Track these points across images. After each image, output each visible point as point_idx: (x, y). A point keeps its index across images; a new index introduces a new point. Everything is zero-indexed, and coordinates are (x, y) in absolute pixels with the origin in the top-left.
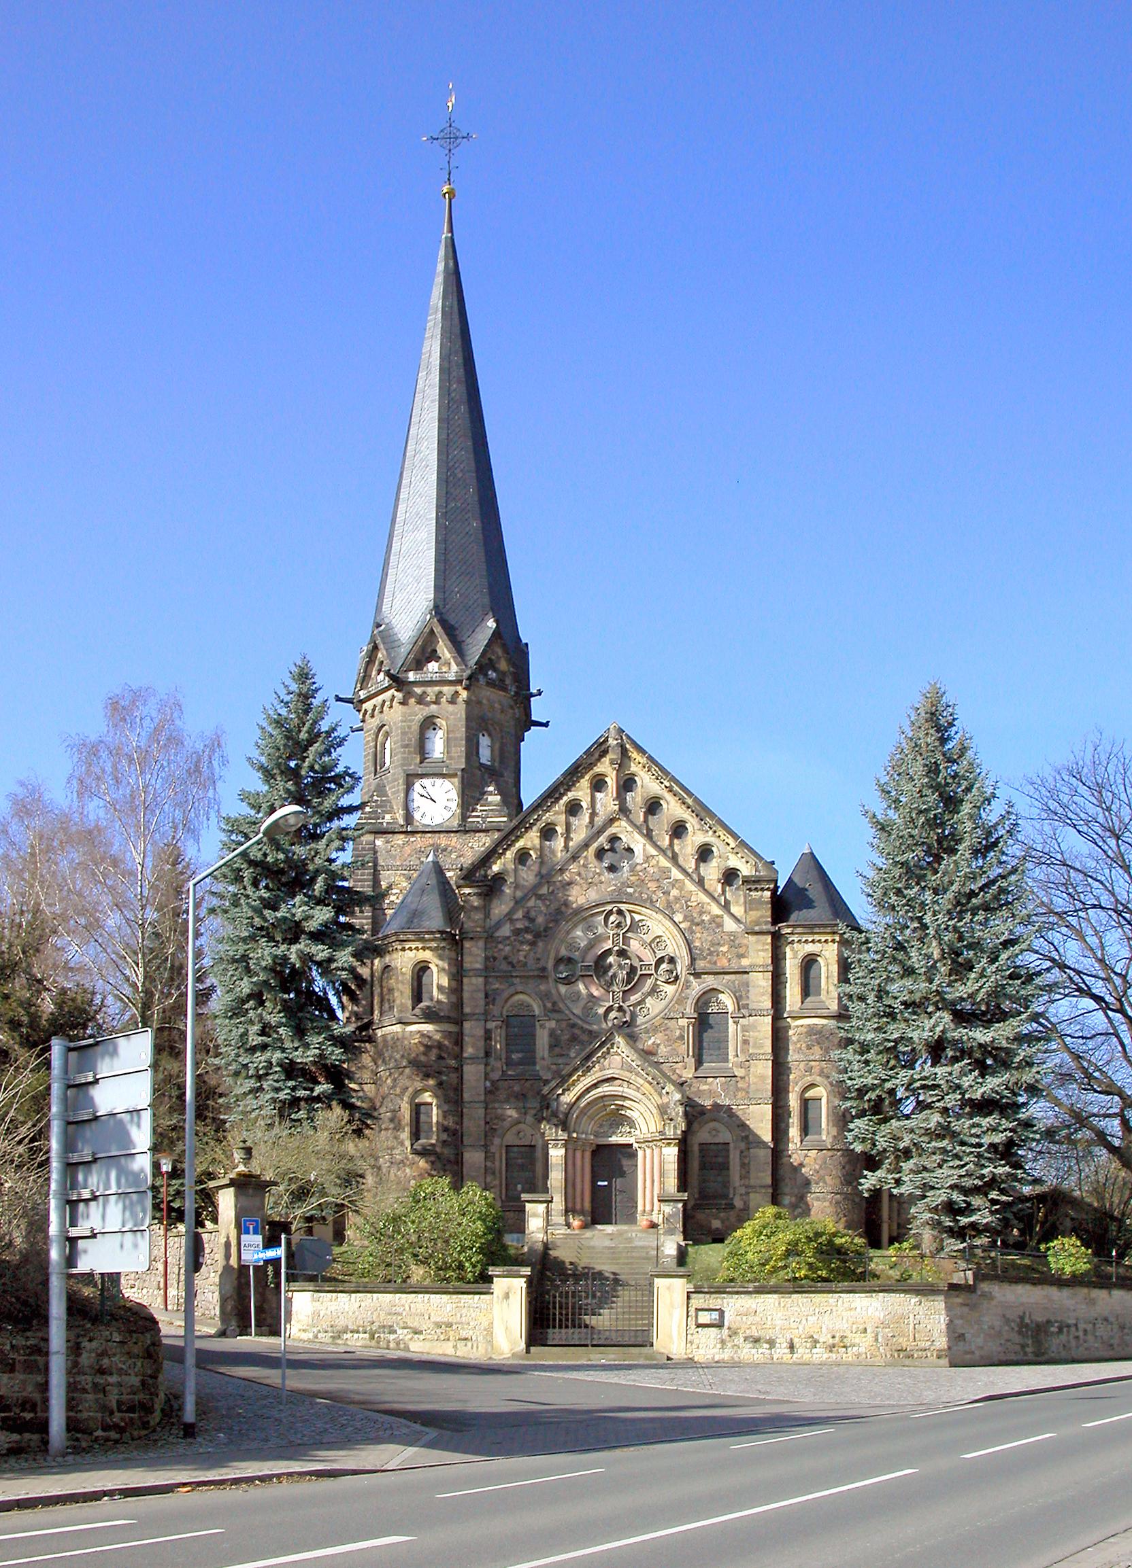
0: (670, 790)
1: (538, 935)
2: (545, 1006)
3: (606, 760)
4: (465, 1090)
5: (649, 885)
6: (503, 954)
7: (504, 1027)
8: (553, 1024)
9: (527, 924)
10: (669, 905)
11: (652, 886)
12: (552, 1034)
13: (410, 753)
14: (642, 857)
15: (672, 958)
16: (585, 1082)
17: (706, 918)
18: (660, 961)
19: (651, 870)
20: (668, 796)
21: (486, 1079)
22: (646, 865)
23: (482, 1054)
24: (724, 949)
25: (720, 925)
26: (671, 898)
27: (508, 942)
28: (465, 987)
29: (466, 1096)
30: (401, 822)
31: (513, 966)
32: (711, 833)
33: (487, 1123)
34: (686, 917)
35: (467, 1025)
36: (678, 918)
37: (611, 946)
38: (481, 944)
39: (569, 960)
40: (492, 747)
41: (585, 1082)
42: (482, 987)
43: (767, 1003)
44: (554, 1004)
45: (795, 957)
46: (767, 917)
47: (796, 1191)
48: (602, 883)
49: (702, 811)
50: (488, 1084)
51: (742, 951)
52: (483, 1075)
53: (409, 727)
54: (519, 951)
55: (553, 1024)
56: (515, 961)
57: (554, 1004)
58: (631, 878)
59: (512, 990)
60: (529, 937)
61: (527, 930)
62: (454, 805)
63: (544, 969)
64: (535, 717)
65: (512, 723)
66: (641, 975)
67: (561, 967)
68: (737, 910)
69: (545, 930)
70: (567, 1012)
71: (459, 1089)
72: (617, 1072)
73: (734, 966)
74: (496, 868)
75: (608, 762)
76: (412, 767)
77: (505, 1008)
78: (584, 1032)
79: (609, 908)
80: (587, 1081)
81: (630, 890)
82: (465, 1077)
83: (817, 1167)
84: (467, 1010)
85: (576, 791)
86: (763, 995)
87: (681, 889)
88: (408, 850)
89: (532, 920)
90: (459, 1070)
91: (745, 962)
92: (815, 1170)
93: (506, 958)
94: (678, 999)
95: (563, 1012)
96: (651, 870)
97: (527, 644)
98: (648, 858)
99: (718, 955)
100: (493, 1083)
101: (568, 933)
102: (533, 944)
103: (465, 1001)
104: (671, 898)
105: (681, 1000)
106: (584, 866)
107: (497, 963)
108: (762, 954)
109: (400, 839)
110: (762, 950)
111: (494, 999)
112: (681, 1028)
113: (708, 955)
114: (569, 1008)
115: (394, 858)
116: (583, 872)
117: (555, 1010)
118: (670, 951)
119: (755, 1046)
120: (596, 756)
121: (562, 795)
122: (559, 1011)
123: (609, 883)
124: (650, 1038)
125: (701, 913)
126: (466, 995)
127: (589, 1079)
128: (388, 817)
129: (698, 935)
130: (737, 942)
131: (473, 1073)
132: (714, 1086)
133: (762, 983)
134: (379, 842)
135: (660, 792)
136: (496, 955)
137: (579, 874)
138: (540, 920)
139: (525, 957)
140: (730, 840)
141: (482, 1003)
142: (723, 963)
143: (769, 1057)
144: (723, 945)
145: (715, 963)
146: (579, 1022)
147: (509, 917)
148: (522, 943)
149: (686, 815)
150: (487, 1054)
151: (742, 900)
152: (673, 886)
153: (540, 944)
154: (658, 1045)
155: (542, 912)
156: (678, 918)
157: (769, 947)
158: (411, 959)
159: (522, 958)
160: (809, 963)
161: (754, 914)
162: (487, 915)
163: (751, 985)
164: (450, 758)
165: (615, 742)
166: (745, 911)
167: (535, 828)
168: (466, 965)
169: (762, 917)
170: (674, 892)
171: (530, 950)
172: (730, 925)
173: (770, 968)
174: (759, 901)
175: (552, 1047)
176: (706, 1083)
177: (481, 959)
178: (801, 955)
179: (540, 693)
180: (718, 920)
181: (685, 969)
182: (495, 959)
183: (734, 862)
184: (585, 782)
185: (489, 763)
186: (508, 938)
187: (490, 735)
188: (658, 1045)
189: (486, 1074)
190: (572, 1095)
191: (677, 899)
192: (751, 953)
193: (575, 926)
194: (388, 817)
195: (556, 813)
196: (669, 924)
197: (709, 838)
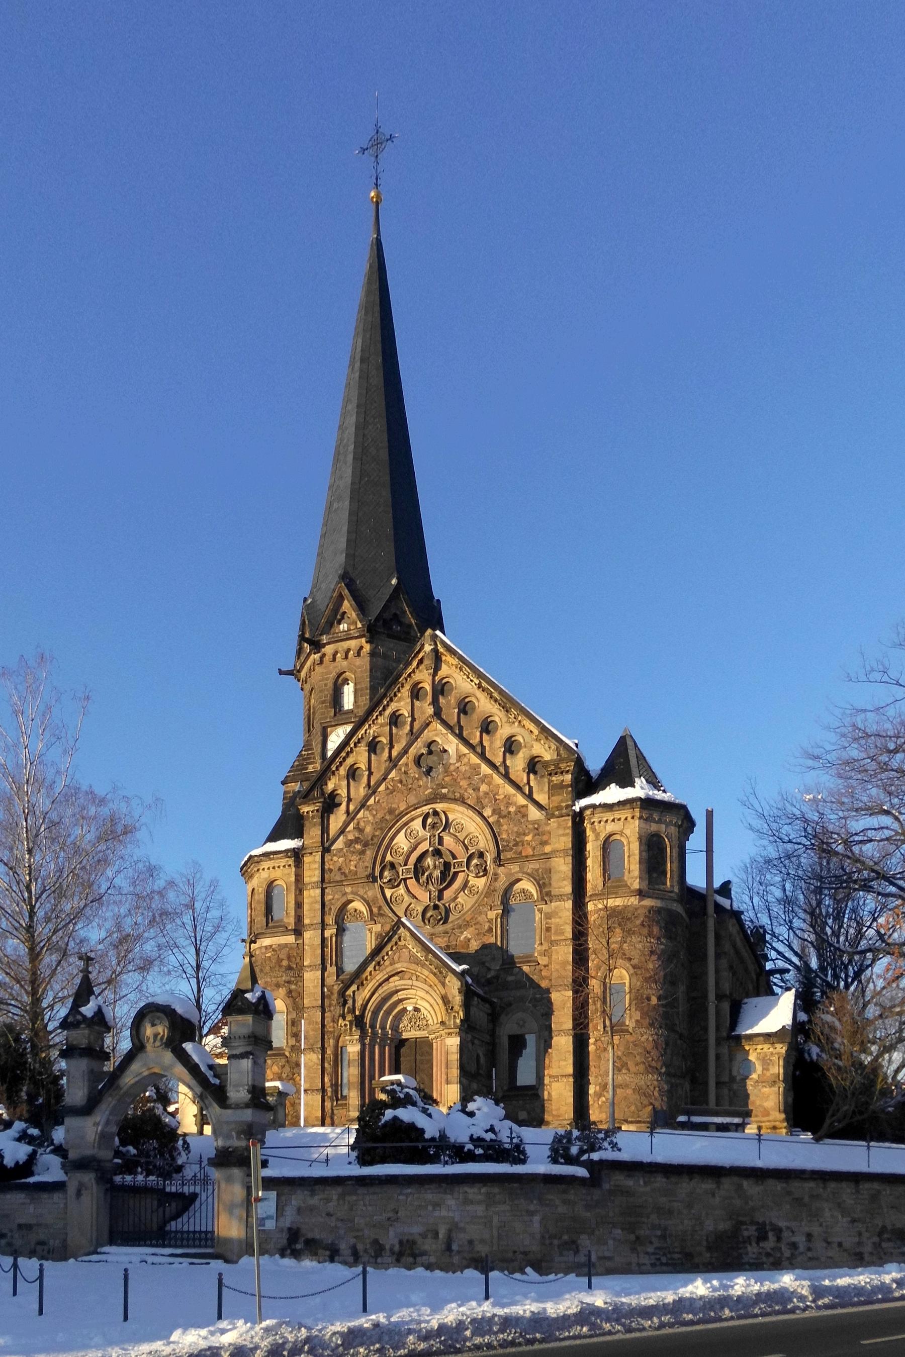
1: (366, 845)
6: (338, 865)
10: (479, 800)
11: (464, 783)
16: (378, 978)
17: (512, 809)
19: (463, 768)
24: (528, 838)
25: (525, 816)
26: (481, 794)
27: (341, 854)
34: (494, 811)
36: (487, 812)
43: (568, 889)
48: (420, 786)
51: (545, 838)
53: (326, 685)
58: (446, 779)
60: (358, 847)
61: (357, 840)
69: (372, 839)
79: (426, 809)
80: (380, 976)
81: (444, 791)
87: (489, 784)
91: (548, 849)
93: (340, 869)
96: (463, 768)
99: (523, 845)
102: (363, 852)
106: (406, 773)
107: (333, 874)
108: (563, 839)
110: (563, 835)
112: (490, 921)
119: (556, 934)
124: (462, 933)
125: (508, 804)
129: (505, 827)
130: (540, 830)
133: (563, 866)
137: (401, 782)
138: (368, 829)
139: (356, 867)
143: (569, 942)
147: (342, 831)
152: (483, 781)
154: (469, 940)
155: (369, 821)
159: (352, 868)
161: (556, 799)
166: (549, 798)
169: (562, 801)
171: (360, 859)
172: (534, 813)
174: (561, 786)
176: (512, 974)
182: (331, 870)
186: (342, 849)
188: (469, 940)
191: (486, 794)
192: (553, 840)
196: (478, 819)
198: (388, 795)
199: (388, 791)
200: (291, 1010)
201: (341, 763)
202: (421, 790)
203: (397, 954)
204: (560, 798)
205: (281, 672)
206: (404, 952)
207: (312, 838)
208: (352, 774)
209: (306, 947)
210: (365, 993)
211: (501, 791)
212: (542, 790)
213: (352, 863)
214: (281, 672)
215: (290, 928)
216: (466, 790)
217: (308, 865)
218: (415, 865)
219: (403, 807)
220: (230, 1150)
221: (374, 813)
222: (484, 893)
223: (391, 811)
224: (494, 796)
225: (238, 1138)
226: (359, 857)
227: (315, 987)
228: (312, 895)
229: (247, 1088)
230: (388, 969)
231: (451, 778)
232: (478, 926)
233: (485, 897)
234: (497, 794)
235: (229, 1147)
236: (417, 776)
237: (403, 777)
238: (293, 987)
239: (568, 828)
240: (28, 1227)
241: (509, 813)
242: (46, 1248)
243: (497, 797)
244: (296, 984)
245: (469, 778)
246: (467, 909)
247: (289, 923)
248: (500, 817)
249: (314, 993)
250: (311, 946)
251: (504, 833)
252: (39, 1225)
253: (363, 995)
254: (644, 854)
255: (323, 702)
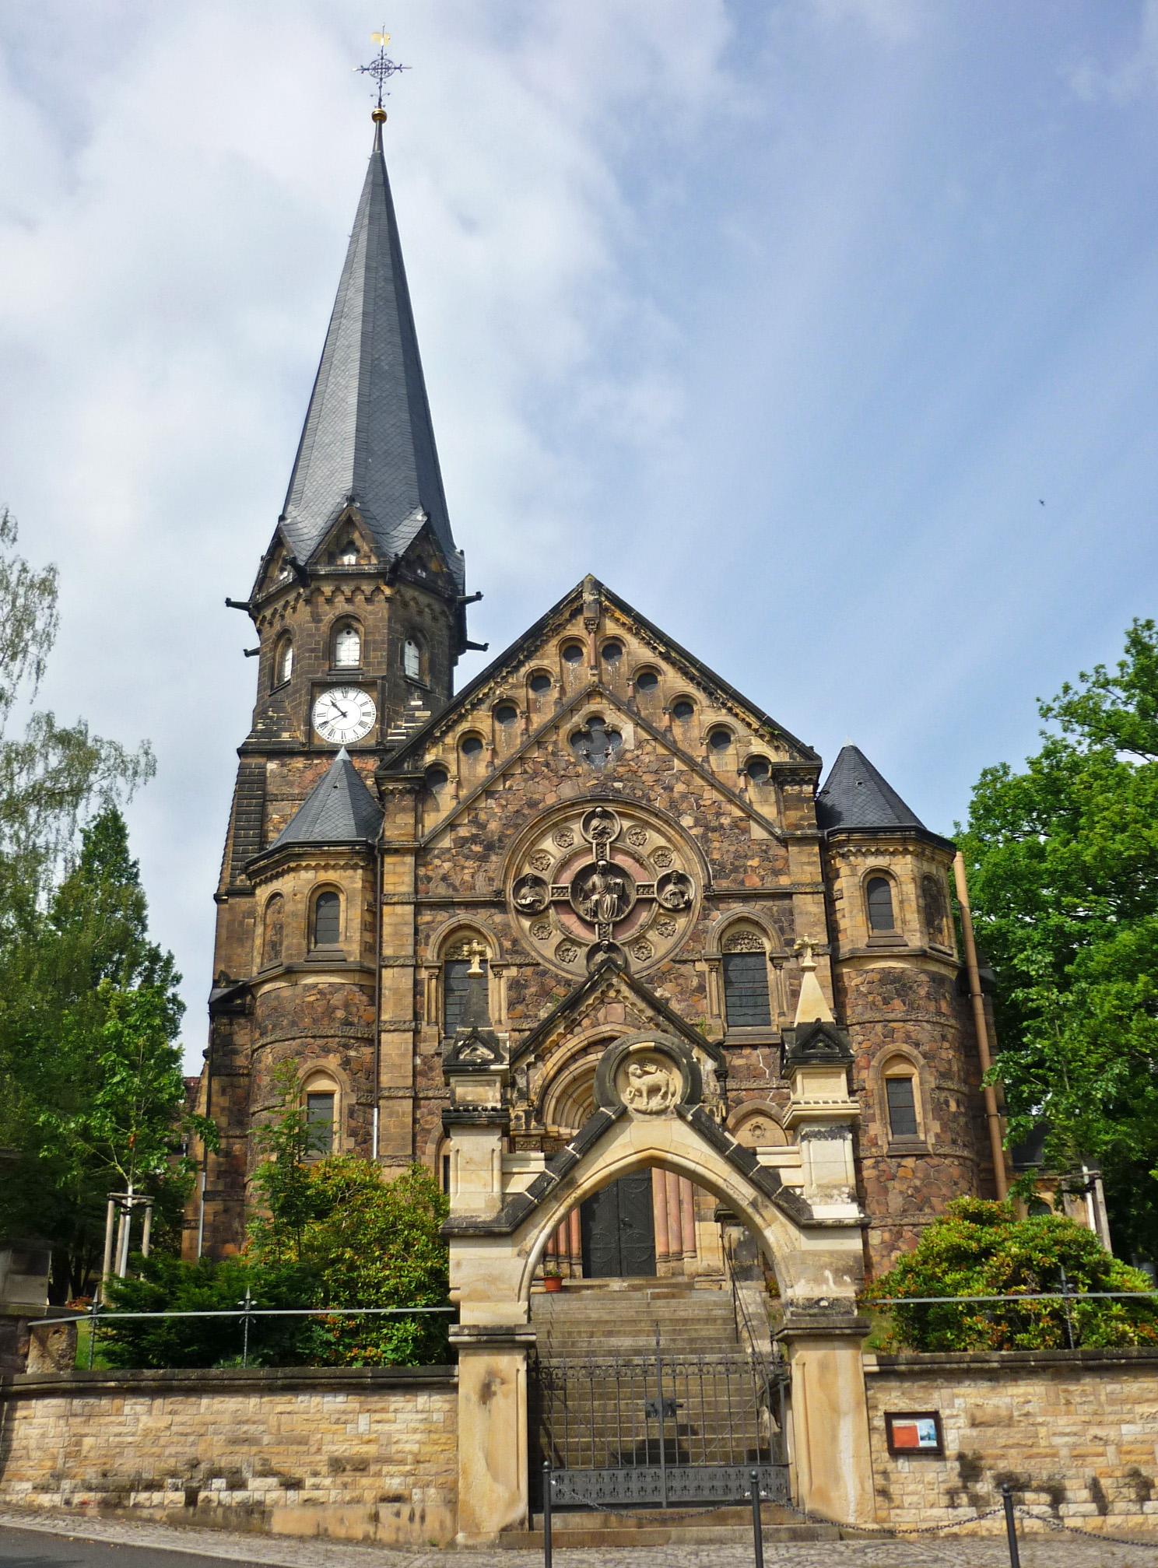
0: (666, 657)
1: (490, 847)
2: (501, 945)
3: (580, 620)
4: (383, 1070)
5: (644, 778)
6: (441, 871)
7: (442, 976)
8: (513, 972)
9: (474, 831)
10: (673, 804)
11: (649, 779)
12: (515, 985)
13: (317, 658)
14: (632, 741)
15: (682, 875)
16: (570, 1045)
17: (726, 821)
18: (664, 881)
20: (664, 665)
21: (415, 1054)
22: (639, 752)
23: (410, 1017)
24: (755, 862)
25: (746, 831)
26: (676, 795)
27: (448, 856)
28: (386, 919)
29: (385, 1079)
30: (303, 739)
31: (455, 889)
32: (724, 711)
33: (415, 1121)
35: (387, 973)
36: (687, 821)
37: (595, 860)
38: (410, 860)
39: (537, 882)
40: (420, 659)
41: (570, 1045)
42: (411, 918)
44: (515, 942)
45: (853, 874)
46: (810, 818)
47: (890, 1221)
49: (711, 683)
50: (418, 1061)
51: (779, 864)
52: (411, 1047)
54: (463, 868)
55: (513, 972)
56: (457, 883)
57: (515, 942)
58: (620, 769)
59: (453, 922)
60: (477, 848)
61: (474, 839)
62: (371, 721)
63: (499, 893)
64: (470, 638)
65: (445, 632)
66: (639, 900)
67: (525, 890)
68: (768, 811)
69: (500, 840)
70: (533, 953)
71: (373, 1072)
72: (618, 1028)
73: (770, 884)
74: (429, 758)
75: (582, 624)
76: (320, 675)
77: (444, 950)
78: (558, 982)
80: (573, 1043)
81: (618, 785)
82: (384, 1049)
83: (918, 1183)
84: (388, 951)
85: (542, 658)
86: (815, 925)
88: (309, 775)
89: (482, 826)
90: (373, 1041)
91: (784, 881)
92: (916, 1188)
93: (444, 878)
94: (693, 933)
95: (529, 954)
97: (462, 552)
98: (639, 745)
99: (745, 872)
100: (425, 1059)
101: (533, 844)
102: (483, 858)
103: (385, 938)
104: (676, 795)
105: (697, 936)
106: (554, 754)
107: (432, 885)
109: (299, 763)
110: (810, 864)
111: (428, 936)
112: (701, 975)
113: (731, 872)
114: (536, 950)
115: (291, 784)
116: (552, 762)
117: (516, 949)
118: (677, 864)
120: (567, 615)
121: (521, 664)
122: (523, 953)
123: (588, 775)
125: (718, 815)
126: (387, 930)
127: (575, 1041)
128: (285, 736)
129: (716, 844)
130: (771, 853)
131: (395, 1046)
132: (753, 1060)
133: (810, 907)
134: (272, 766)
135: (653, 660)
136: (430, 873)
137: (547, 765)
138: (493, 826)
139: (473, 877)
140: (752, 719)
141: (411, 940)
142: (753, 882)
144: (752, 858)
145: (742, 882)
146: (553, 968)
148: (467, 858)
149: (690, 689)
150: (417, 1016)
151: (773, 798)
152: (678, 779)
153: (494, 858)
156: (687, 821)
157: (817, 859)
158: (308, 881)
159: (467, 878)
160: (877, 881)
161: (793, 815)
162: (418, 820)
163: (796, 912)
164: (367, 664)
165: (592, 598)
166: (779, 812)
167: (484, 707)
168: (388, 888)
169: (802, 818)
170: (680, 788)
171: (480, 867)
172: (758, 833)
173: (822, 888)
174: (800, 799)
175: (511, 1005)
177: (409, 879)
178: (861, 871)
179: (479, 596)
180: (742, 824)
181: (700, 891)
182: (429, 879)
183: (759, 747)
184: (552, 648)
185: (416, 677)
186: (450, 849)
187: (419, 646)
189: (415, 1046)
190: (549, 1065)
193: (543, 834)
194: (285, 736)
195: (514, 686)
197: (723, 717)
198: (526, 781)
199: (526, 776)
200: (349, 1091)
201: (450, 728)
202: (580, 780)
203: (603, 1010)
204: (799, 814)
205: (229, 603)
206: (615, 1008)
207: (399, 827)
208: (471, 743)
209: (386, 992)
210: (550, 1066)
211: (706, 795)
212: (766, 801)
213: (466, 871)
214: (229, 603)
215: (352, 959)
216: (651, 788)
217: (392, 867)
218: (574, 883)
219: (551, 800)
220: (824, 1303)
221: (504, 803)
222: (689, 934)
223: (532, 804)
224: (696, 801)
225: (838, 1281)
226: (478, 863)
227: (403, 1055)
228: (396, 918)
229: (846, 1190)
230: (590, 1032)
231: (627, 768)
232: (680, 981)
233: (690, 939)
234: (701, 797)
235: (822, 1299)
236: (572, 760)
237: (550, 757)
238: (352, 1053)
239: (815, 855)
240: (361, 1466)
241: (721, 826)
242: (406, 1510)
243: (702, 803)
244: (356, 1050)
245: (656, 772)
246: (657, 957)
247: (350, 953)
248: (707, 828)
249: (400, 1066)
250: (396, 991)
251: (715, 852)
252: (388, 1460)
253: (544, 1071)
254: (920, 900)
255: (312, 650)
